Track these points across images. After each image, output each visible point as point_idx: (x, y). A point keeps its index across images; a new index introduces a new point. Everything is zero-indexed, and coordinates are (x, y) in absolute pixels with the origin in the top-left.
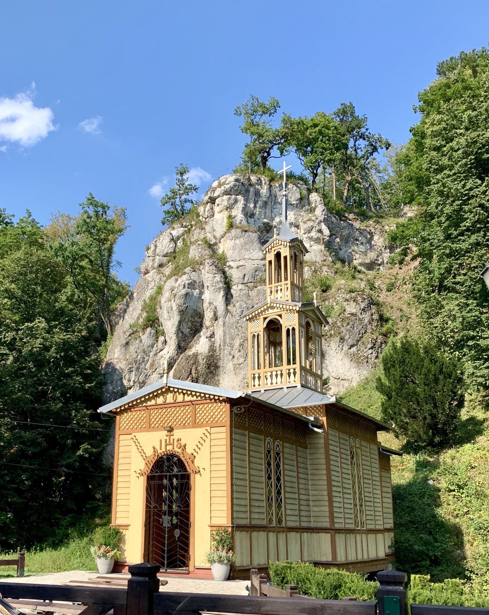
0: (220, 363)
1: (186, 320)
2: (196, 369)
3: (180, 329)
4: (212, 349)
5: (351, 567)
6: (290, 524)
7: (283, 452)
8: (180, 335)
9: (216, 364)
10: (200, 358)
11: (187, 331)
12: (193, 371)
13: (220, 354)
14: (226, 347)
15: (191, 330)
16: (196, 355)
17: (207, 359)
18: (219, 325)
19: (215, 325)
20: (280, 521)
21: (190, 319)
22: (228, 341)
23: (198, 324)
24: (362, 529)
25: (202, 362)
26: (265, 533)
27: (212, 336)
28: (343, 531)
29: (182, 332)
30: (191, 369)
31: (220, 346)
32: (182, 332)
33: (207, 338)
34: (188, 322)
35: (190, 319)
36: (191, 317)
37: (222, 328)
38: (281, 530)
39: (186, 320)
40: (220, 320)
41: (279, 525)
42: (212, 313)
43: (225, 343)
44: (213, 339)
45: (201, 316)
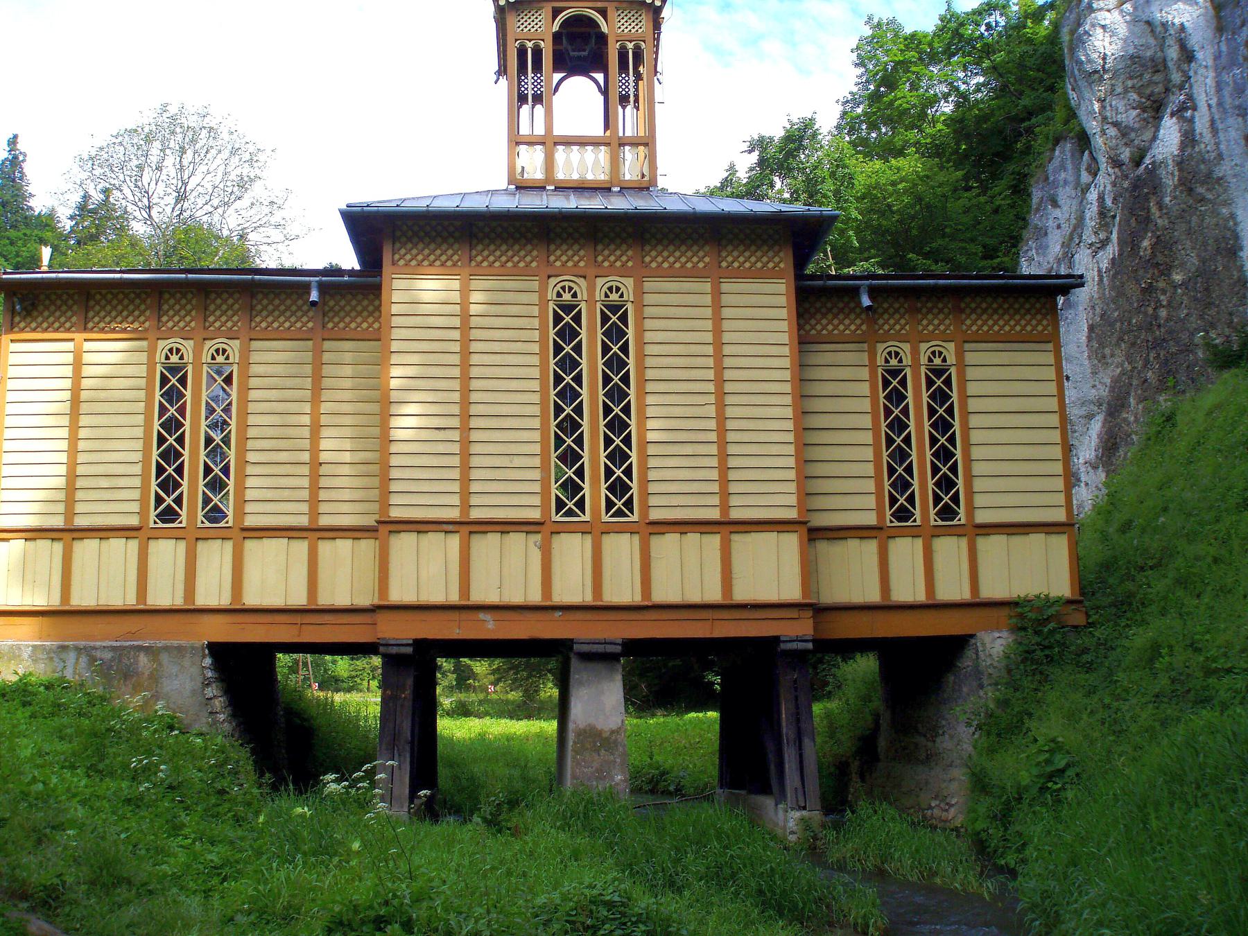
0: (1224, 169)
1: (1119, 90)
2: (1160, 207)
3: (1104, 119)
4: (1189, 138)
5: (482, 616)
6: (250, 521)
7: (245, 363)
8: (1112, 131)
9: (1209, 175)
10: (1162, 172)
11: (1130, 117)
12: (1154, 210)
13: (1217, 144)
14: (1231, 121)
15: (1144, 110)
16: (1153, 171)
17: (1180, 170)
18: (1202, 71)
19: (1191, 73)
20: (215, 514)
21: (1130, 83)
22: (1228, 100)
23: (1159, 89)
24: (606, 518)
25: (1170, 180)
26: (133, 545)
27: (1190, 104)
28: (450, 527)
29: (1116, 124)
30: (1148, 210)
31: (1213, 122)
32: (1116, 124)
33: (1172, 115)
34: (1126, 91)
35: (1130, 83)
36: (1131, 78)
37: (1211, 74)
38: (212, 533)
39: (1119, 90)
40: (1204, 56)
41: (208, 524)
42: (1176, 47)
43: (1225, 111)
44: (1189, 113)
45: (1159, 66)
